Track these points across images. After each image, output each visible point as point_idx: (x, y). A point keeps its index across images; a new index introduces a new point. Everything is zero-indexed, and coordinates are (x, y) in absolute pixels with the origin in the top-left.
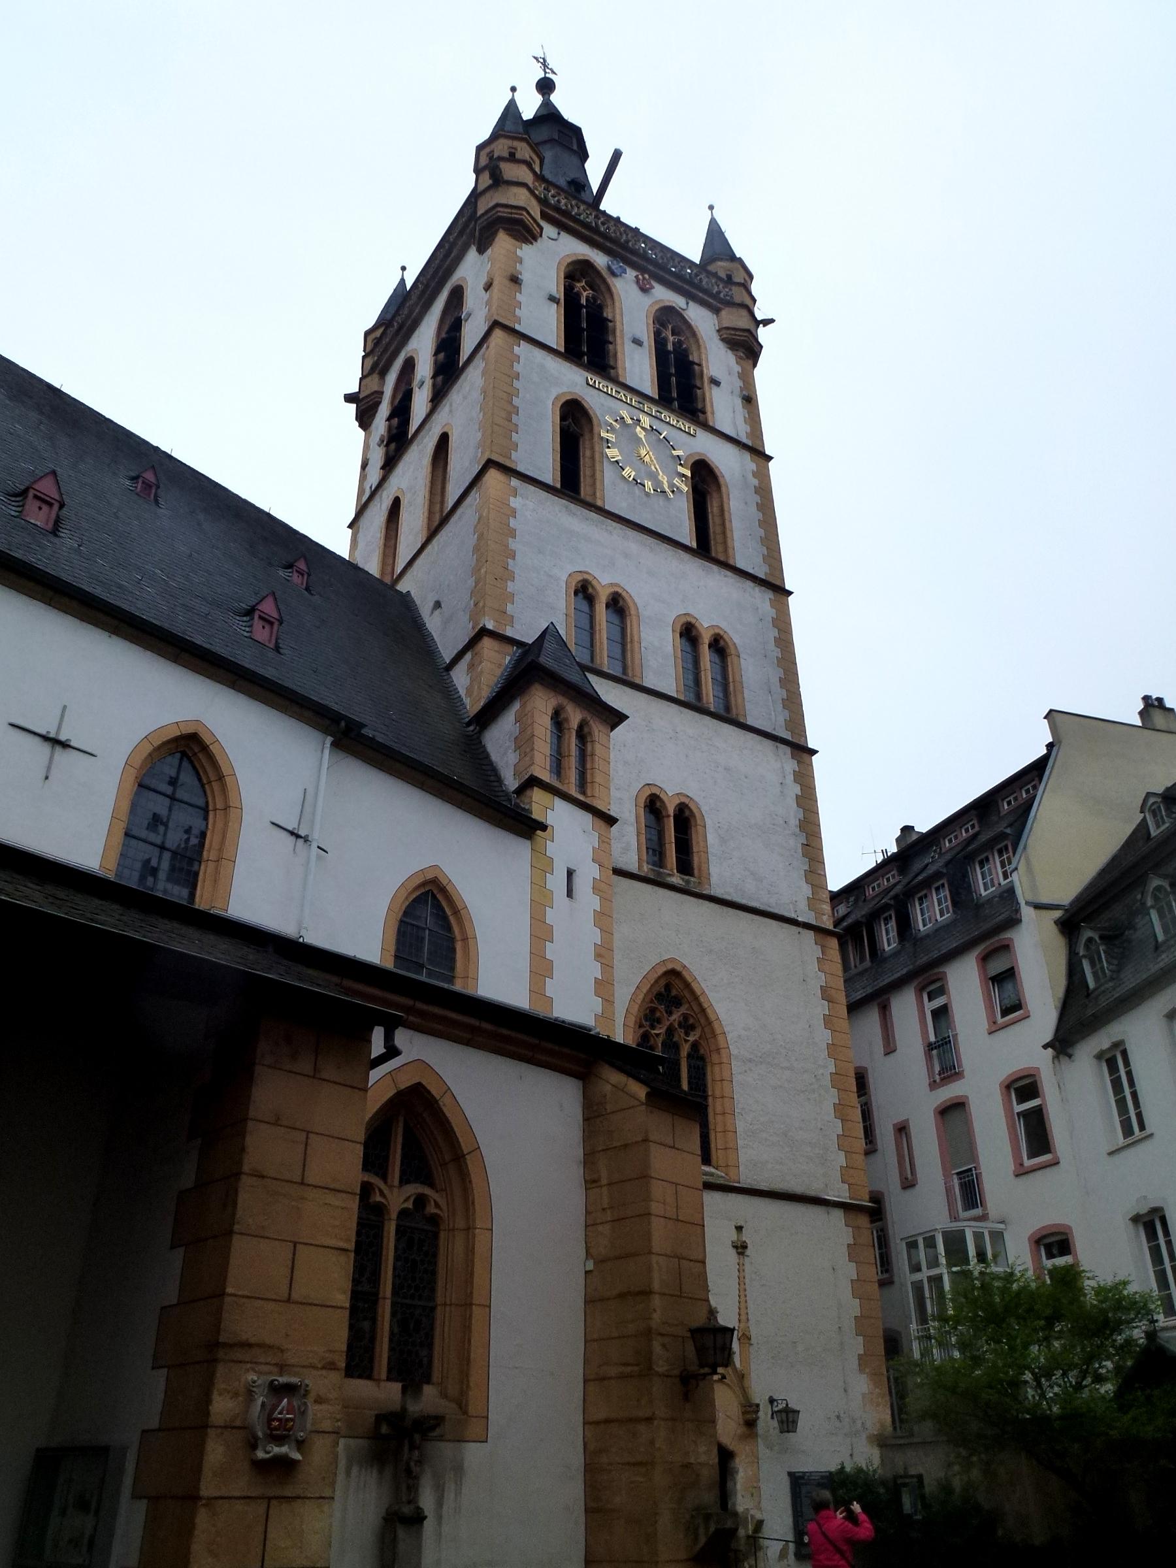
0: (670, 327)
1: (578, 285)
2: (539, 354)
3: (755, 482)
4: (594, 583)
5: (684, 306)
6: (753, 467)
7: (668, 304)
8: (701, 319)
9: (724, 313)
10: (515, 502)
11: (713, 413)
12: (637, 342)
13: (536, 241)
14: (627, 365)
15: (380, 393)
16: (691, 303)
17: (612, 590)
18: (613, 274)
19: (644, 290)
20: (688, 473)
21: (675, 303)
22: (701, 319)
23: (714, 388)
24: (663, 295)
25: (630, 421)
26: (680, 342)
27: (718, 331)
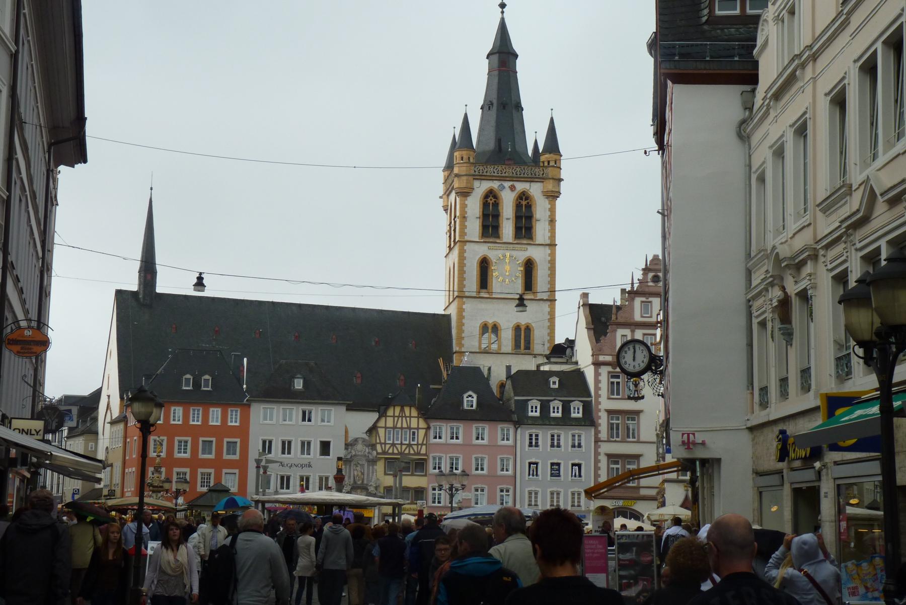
0: (524, 198)
1: (489, 200)
2: (472, 245)
3: (549, 258)
4: (488, 324)
5: (528, 189)
6: (549, 251)
7: (522, 191)
8: (535, 190)
9: (545, 183)
10: (464, 307)
11: (535, 235)
12: (507, 219)
13: (472, 193)
14: (504, 231)
15: (448, 206)
16: (532, 184)
17: (493, 324)
18: (501, 191)
19: (512, 188)
20: (522, 269)
21: (525, 188)
22: (535, 190)
23: (538, 223)
24: (520, 186)
25: (502, 258)
26: (528, 203)
27: (543, 192)
